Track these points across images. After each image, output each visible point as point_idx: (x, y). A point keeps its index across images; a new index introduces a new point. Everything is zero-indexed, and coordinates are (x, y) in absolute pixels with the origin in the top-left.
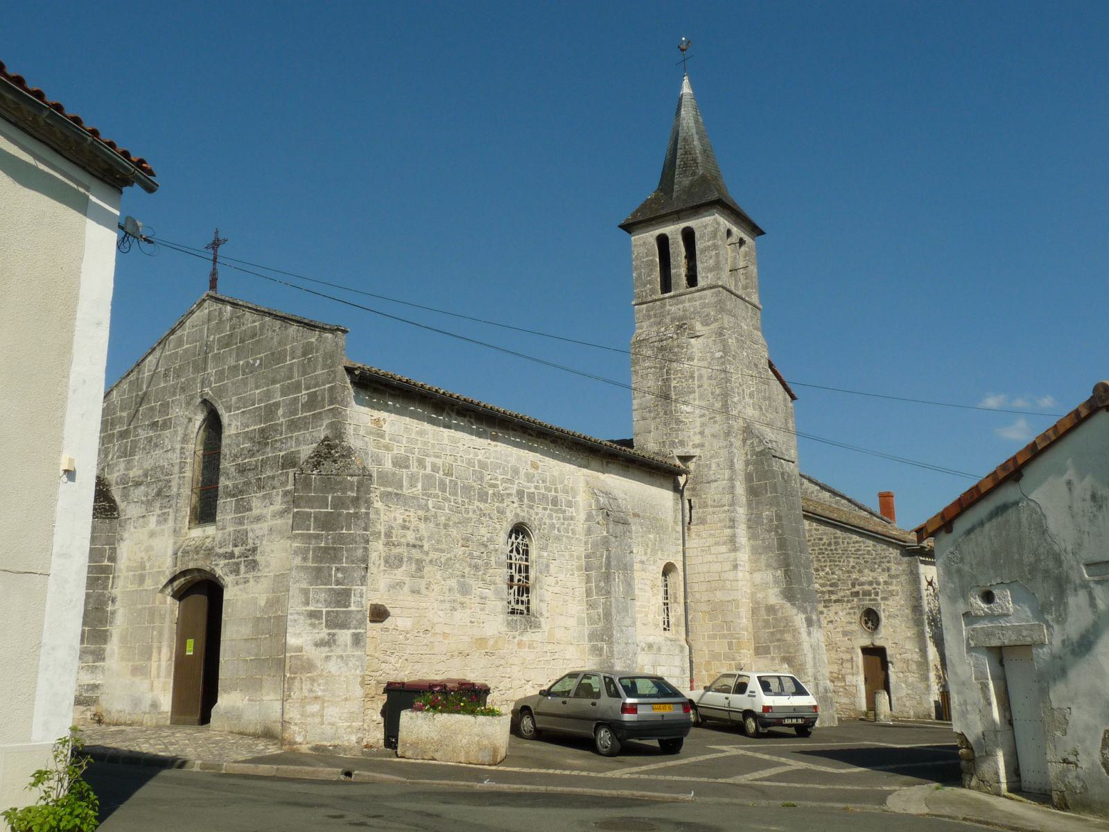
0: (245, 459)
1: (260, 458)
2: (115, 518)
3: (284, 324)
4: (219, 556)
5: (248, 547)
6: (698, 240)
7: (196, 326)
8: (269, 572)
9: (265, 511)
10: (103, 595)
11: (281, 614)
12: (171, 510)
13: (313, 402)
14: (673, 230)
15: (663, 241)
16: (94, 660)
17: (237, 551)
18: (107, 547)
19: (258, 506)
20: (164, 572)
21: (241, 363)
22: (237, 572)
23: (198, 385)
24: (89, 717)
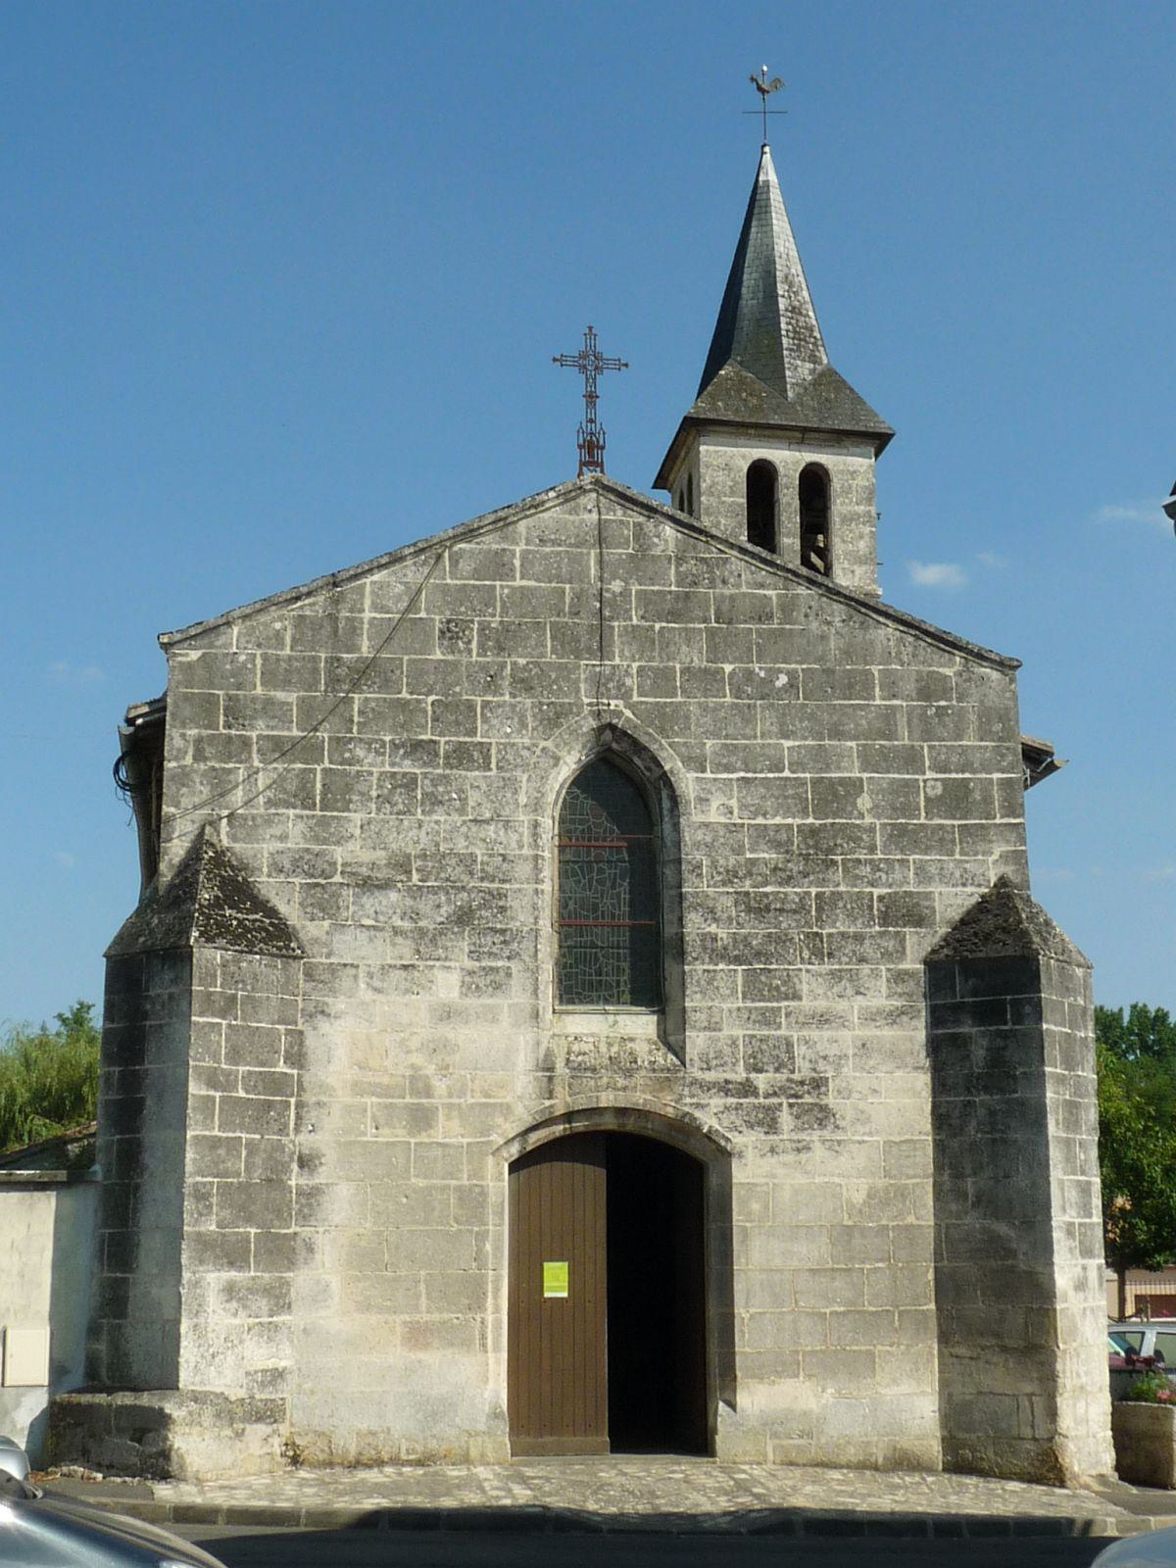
0: (766, 884)
1: (814, 891)
2: (295, 958)
3: (857, 617)
4: (707, 1087)
5: (796, 1076)
6: (838, 496)
7: (554, 543)
8: (870, 1134)
9: (841, 1006)
10: (280, 1147)
11: (915, 1222)
12: (515, 966)
13: (955, 799)
14: (789, 461)
15: (761, 477)
16: (271, 1310)
17: (761, 1081)
18: (282, 1028)
19: (821, 992)
20: (506, 1110)
21: (728, 668)
22: (772, 1126)
23: (582, 686)
24: (279, 1452)
